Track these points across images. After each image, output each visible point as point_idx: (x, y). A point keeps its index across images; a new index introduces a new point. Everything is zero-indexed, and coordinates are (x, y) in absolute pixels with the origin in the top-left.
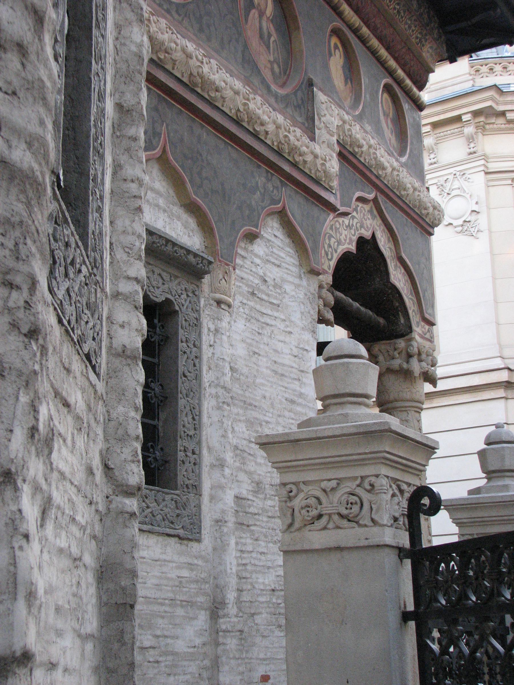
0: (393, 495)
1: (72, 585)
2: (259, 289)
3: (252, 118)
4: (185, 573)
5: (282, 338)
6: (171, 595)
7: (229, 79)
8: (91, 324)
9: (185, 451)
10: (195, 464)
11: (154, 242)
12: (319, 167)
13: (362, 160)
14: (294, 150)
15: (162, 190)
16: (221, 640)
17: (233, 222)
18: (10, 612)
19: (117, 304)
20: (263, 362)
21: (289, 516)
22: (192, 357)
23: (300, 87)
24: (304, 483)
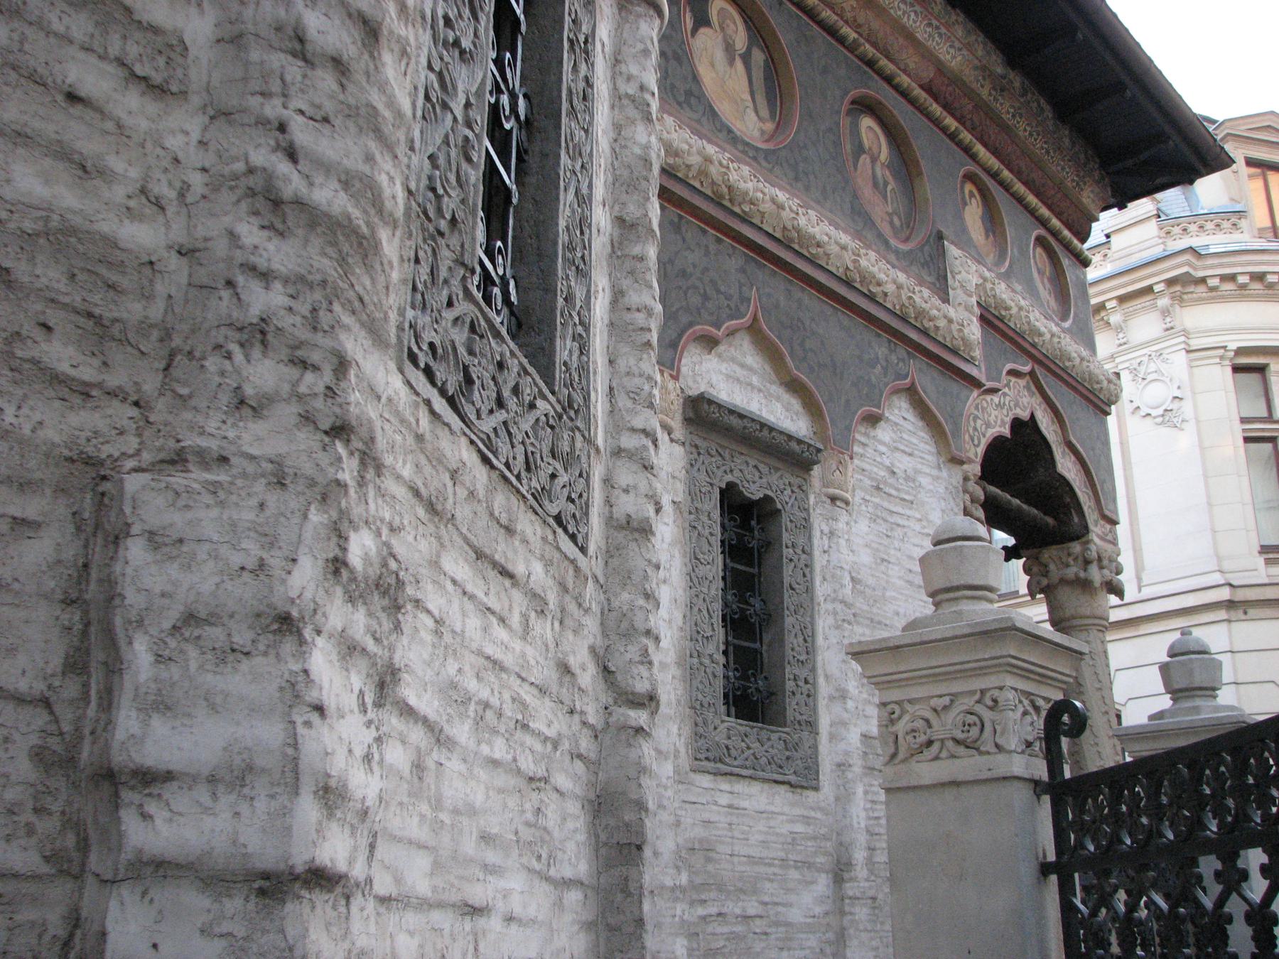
0: (1025, 713)
1: (523, 812)
2: (885, 483)
3: (866, 277)
4: (799, 828)
5: (916, 541)
6: (782, 854)
7: (832, 230)
8: (563, 478)
9: (795, 679)
10: (809, 696)
11: (745, 428)
12: (955, 334)
13: (1012, 325)
14: (921, 314)
15: (755, 366)
16: (847, 909)
17: (848, 401)
18: (285, 812)
19: (619, 463)
20: (895, 571)
21: (892, 744)
22: (801, 564)
23: (928, 241)
24: (909, 701)
